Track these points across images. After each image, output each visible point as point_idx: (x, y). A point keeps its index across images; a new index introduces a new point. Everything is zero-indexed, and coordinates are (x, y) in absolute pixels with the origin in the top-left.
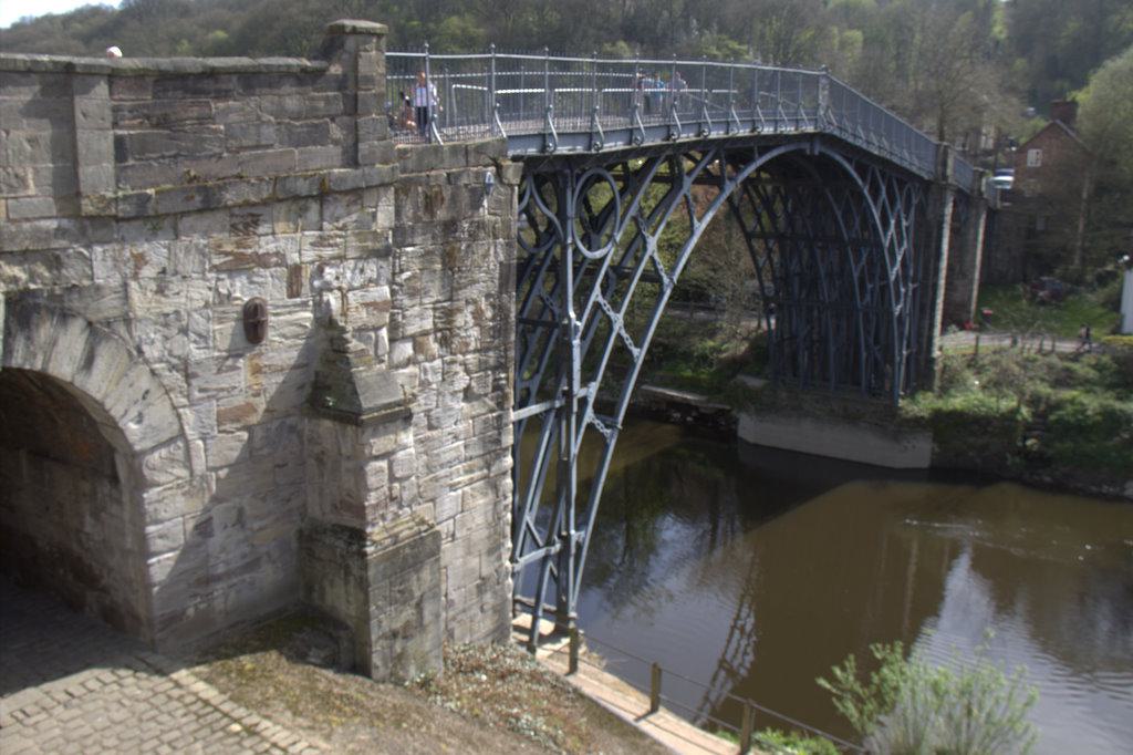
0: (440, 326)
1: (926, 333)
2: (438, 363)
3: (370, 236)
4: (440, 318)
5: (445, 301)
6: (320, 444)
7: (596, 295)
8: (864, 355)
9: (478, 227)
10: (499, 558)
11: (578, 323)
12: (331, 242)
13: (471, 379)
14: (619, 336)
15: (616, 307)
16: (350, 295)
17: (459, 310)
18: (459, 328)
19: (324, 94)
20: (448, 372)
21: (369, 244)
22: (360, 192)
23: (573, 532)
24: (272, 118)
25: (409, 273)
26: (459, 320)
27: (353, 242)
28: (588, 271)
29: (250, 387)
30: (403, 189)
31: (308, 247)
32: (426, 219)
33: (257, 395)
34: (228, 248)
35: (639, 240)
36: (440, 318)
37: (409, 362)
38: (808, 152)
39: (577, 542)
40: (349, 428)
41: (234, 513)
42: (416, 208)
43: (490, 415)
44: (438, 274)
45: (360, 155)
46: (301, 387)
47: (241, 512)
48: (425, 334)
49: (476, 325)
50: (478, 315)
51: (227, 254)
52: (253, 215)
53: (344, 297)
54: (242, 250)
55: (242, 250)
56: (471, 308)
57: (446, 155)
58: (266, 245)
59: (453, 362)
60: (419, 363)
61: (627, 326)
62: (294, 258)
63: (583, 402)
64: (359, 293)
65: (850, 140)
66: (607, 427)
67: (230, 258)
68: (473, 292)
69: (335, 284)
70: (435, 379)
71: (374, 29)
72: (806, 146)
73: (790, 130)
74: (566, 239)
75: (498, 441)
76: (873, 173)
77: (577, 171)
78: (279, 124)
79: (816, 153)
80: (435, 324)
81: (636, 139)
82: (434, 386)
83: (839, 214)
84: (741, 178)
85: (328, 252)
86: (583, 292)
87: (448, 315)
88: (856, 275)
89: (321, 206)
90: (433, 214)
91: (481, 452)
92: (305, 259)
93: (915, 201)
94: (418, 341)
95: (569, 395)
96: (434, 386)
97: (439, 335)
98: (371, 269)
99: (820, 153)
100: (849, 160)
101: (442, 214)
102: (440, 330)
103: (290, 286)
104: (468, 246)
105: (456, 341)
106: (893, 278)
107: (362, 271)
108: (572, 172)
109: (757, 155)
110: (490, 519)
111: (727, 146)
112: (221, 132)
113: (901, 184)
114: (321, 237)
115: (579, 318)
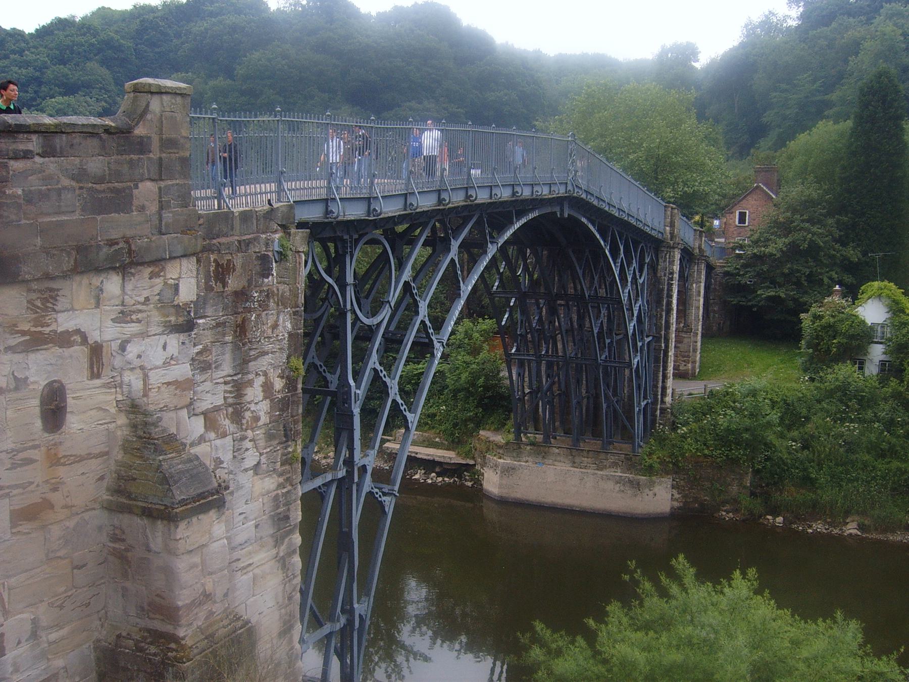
0: (230, 401)
1: (660, 384)
2: (229, 439)
3: (172, 310)
4: (230, 392)
5: (235, 375)
6: (123, 540)
7: (374, 361)
8: (604, 406)
9: (267, 296)
10: (291, 641)
11: (358, 391)
12: (134, 317)
13: (261, 454)
14: (394, 401)
15: (389, 366)
16: (151, 374)
17: (250, 383)
18: (249, 403)
19: (128, 157)
20: (239, 450)
21: (173, 319)
22: (163, 263)
23: (356, 606)
24: (74, 184)
25: (201, 347)
27: (156, 317)
28: (365, 335)
29: (47, 482)
30: (198, 255)
31: (110, 322)
32: (218, 287)
33: (55, 489)
34: (25, 327)
35: (408, 300)
36: (230, 392)
38: (559, 216)
39: (360, 615)
40: (159, 522)
41: (28, 627)
43: (279, 492)
44: (229, 348)
45: (163, 223)
46: (102, 478)
47: (35, 622)
48: (217, 409)
49: (265, 398)
51: (24, 333)
52: (51, 290)
53: (146, 378)
54: (39, 329)
55: (39, 329)
56: (262, 379)
57: (237, 223)
58: (65, 322)
59: (243, 438)
60: (210, 441)
61: (401, 390)
63: (363, 469)
64: (161, 372)
65: (595, 203)
66: (385, 494)
67: (27, 338)
68: (264, 363)
69: (137, 363)
70: (227, 457)
71: (180, 88)
72: (557, 209)
73: (544, 192)
74: (345, 306)
75: (287, 518)
76: (613, 235)
77: (356, 236)
78: (81, 188)
79: (566, 215)
80: (225, 398)
81: (411, 204)
82: (225, 465)
83: (580, 272)
84: (501, 242)
86: (361, 356)
87: (238, 388)
88: (596, 331)
89: (123, 279)
90: (225, 284)
91: (272, 532)
92: (107, 336)
93: (647, 260)
95: (349, 462)
96: (225, 465)
97: (230, 410)
98: (174, 342)
100: (594, 225)
101: (233, 283)
102: (230, 405)
103: (92, 367)
104: (258, 316)
105: (248, 415)
106: (630, 332)
107: (164, 348)
108: (351, 237)
110: (281, 600)
112: (19, 197)
113: (636, 244)
114: (122, 312)
115: (358, 387)
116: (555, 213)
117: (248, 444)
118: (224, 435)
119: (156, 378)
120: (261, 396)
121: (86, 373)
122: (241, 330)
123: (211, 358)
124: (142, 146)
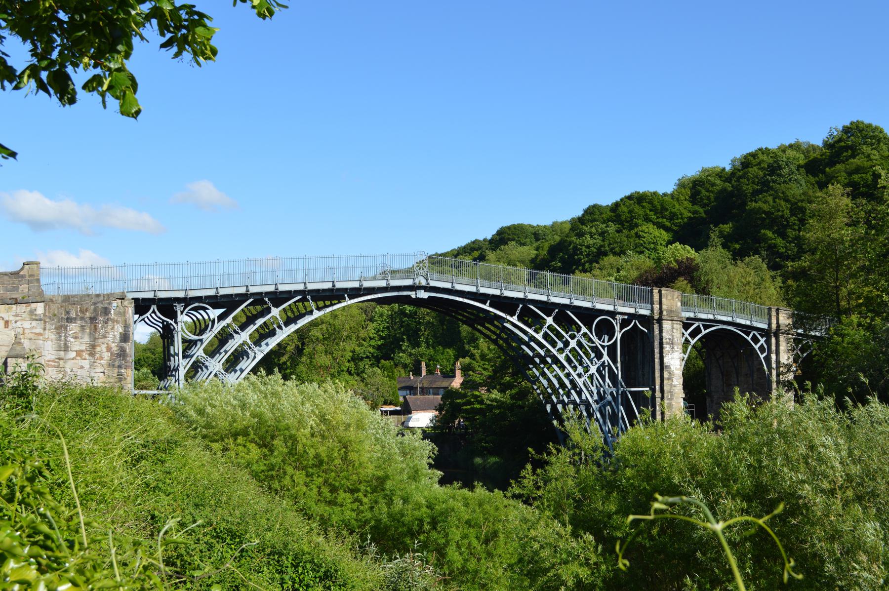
9: (108, 319)
26: (98, 349)
37: (73, 359)
38: (414, 296)
42: (77, 312)
48: (82, 351)
50: (109, 349)
56: (106, 345)
62: (6, 318)
68: (106, 340)
85: (18, 318)
94: (79, 353)
98: (34, 323)
99: (430, 297)
100: (485, 303)
105: (98, 355)
109: (347, 298)
111: (314, 295)
116: (409, 296)
117: (96, 364)
118: (85, 359)
119: (27, 331)
120: (105, 350)
121: (3, 326)
122: (96, 328)
123: (80, 335)
124: (23, 276)
